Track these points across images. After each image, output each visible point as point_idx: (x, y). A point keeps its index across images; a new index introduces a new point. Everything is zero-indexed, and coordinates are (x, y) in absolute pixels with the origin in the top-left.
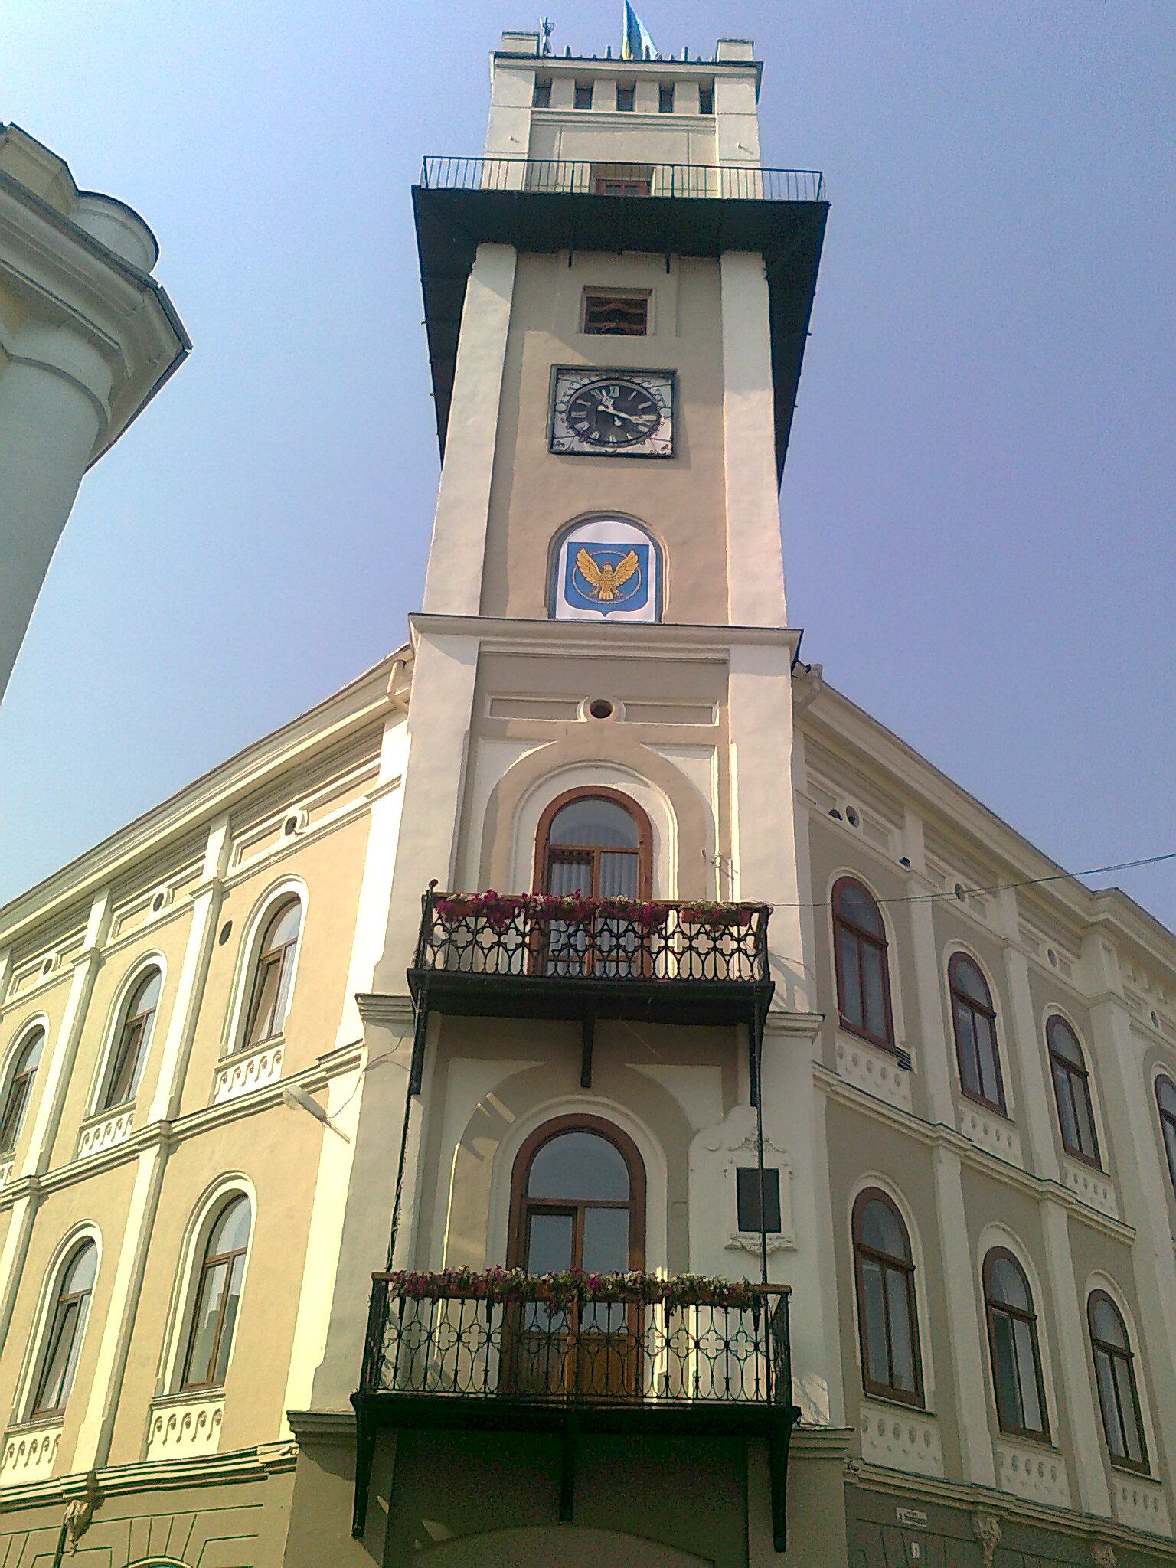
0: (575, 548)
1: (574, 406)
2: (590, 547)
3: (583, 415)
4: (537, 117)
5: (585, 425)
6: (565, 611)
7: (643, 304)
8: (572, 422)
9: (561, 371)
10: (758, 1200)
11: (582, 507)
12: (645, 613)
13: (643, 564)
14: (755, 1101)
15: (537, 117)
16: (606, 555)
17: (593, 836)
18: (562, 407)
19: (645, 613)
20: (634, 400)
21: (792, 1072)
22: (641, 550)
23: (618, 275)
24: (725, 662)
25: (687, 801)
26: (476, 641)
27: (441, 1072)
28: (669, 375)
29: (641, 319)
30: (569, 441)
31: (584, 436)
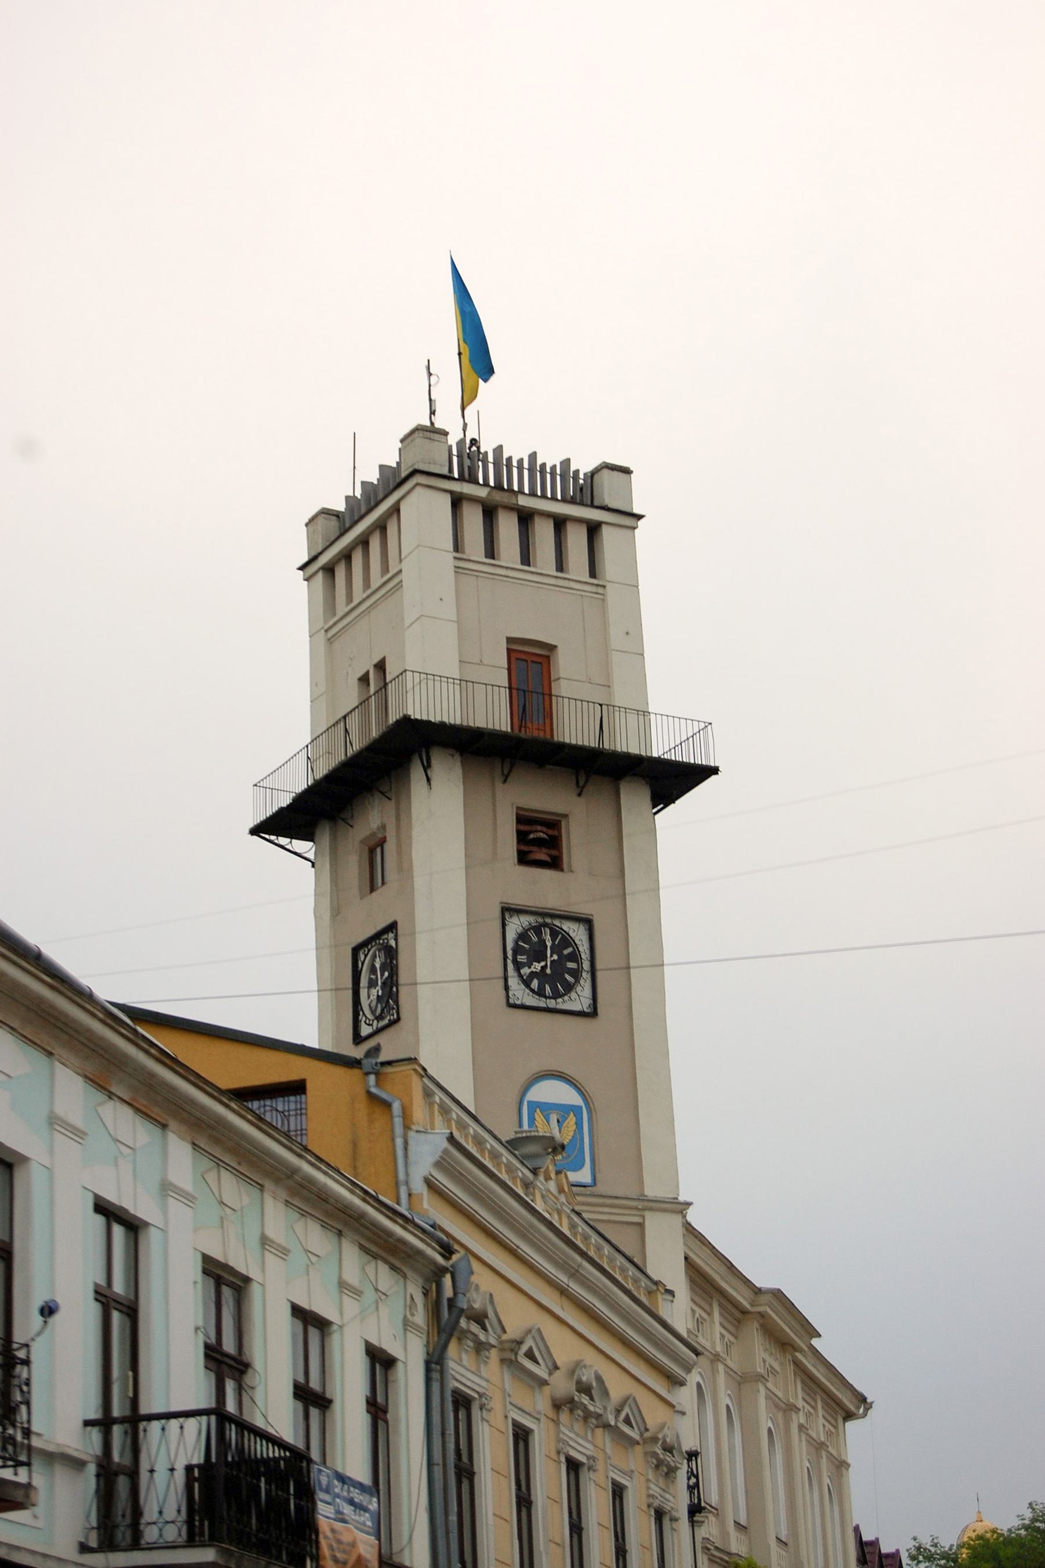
0: (534, 1106)
9: (508, 911)
13: (579, 1124)
22: (576, 1110)
24: (641, 1226)
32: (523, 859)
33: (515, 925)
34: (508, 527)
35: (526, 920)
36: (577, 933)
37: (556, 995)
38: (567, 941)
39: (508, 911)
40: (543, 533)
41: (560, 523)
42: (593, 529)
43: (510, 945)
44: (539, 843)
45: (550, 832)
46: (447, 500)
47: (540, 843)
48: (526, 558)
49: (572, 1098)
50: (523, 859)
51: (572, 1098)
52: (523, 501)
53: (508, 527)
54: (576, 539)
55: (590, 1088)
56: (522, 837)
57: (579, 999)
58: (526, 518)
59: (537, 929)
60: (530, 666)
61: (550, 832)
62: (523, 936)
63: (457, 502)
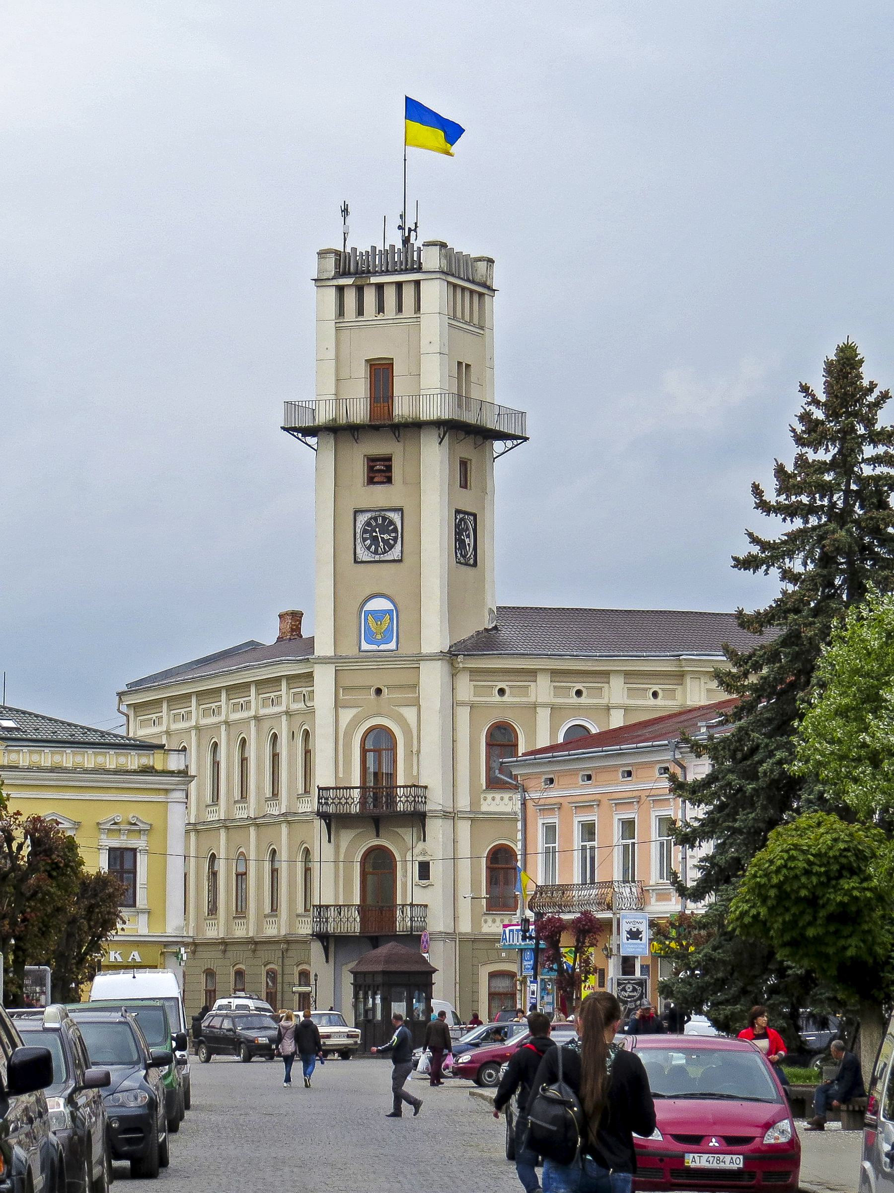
0: (368, 613)
1: (365, 531)
2: (372, 613)
3: (367, 535)
4: (338, 325)
5: (368, 542)
6: (365, 646)
7: (389, 459)
8: (364, 540)
10: (424, 870)
11: (368, 592)
12: (392, 645)
13: (391, 619)
14: (424, 841)
15: (338, 325)
16: (378, 615)
17: (379, 744)
18: (358, 536)
19: (392, 645)
20: (388, 526)
21: (436, 828)
22: (390, 612)
23: (379, 447)
25: (407, 731)
26: (333, 666)
27: (337, 833)
28: (400, 510)
29: (389, 469)
30: (363, 555)
31: (368, 548)
32: (371, 481)
33: (362, 519)
34: (370, 296)
35: (369, 515)
36: (395, 517)
37: (385, 552)
38: (391, 523)
39: (357, 512)
40: (390, 295)
41: (399, 285)
42: (417, 283)
43: (358, 530)
44: (380, 471)
45: (387, 463)
46: (333, 291)
47: (379, 471)
48: (381, 309)
49: (390, 606)
50: (371, 481)
51: (390, 606)
52: (374, 280)
53: (370, 296)
54: (408, 293)
55: (396, 600)
56: (371, 469)
57: (395, 553)
58: (380, 287)
59: (375, 519)
60: (381, 373)
61: (387, 463)
62: (368, 524)
63: (340, 289)
